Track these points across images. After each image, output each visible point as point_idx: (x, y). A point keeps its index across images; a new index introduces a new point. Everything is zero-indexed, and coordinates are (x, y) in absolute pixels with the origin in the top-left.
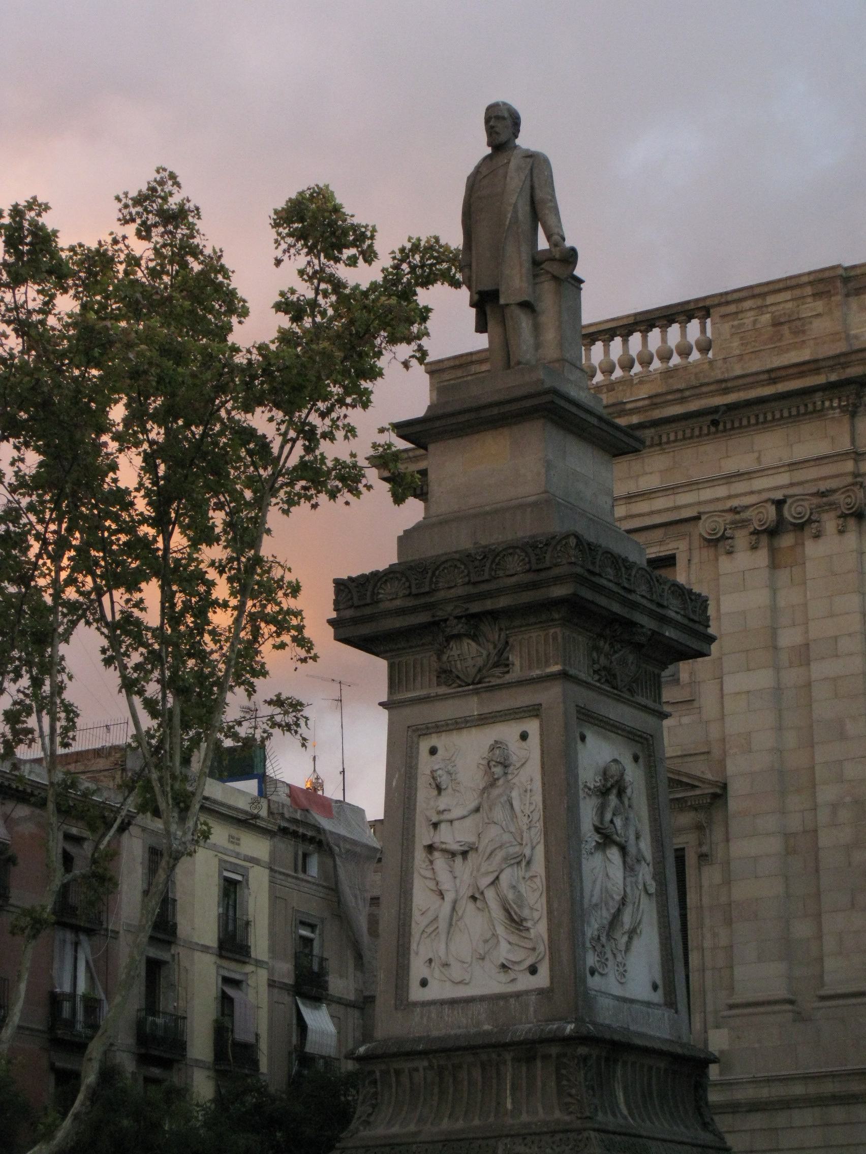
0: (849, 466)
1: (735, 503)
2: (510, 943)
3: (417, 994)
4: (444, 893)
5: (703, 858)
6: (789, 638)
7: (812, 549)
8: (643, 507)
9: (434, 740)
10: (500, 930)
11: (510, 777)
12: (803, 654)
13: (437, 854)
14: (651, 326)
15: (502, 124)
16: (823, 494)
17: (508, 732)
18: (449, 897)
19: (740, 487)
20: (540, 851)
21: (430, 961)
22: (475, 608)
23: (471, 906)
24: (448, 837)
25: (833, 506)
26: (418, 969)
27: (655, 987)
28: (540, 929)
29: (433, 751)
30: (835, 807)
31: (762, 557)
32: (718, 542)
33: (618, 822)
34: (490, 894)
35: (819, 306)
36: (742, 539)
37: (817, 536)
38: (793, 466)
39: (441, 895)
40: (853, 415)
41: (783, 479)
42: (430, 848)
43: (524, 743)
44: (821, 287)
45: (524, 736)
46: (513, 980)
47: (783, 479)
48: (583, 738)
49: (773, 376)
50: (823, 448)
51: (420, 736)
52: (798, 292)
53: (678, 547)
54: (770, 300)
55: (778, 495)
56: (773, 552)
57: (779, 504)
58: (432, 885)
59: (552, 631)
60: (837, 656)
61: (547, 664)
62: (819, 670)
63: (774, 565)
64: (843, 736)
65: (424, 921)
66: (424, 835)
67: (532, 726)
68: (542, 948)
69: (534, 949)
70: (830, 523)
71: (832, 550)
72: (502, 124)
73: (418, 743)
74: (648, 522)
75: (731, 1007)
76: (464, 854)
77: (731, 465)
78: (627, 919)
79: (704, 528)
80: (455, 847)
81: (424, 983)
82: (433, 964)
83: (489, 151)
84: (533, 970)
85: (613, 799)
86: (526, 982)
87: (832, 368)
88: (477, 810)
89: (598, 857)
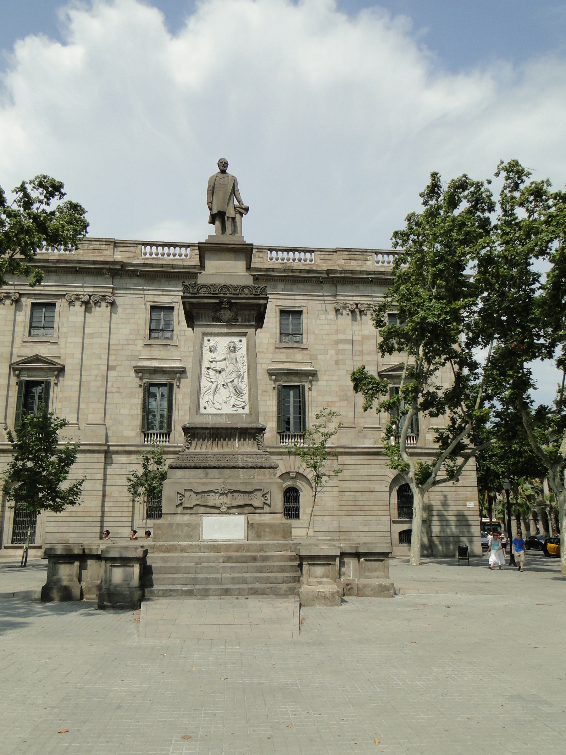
1: (77, 293)
3: (202, 410)
5: (56, 384)
10: (232, 395)
13: (210, 370)
15: (223, 166)
16: (103, 296)
17: (236, 339)
18: (215, 384)
20: (246, 375)
22: (233, 301)
23: (222, 388)
24: (218, 366)
25: (105, 299)
26: (203, 403)
28: (246, 397)
29: (209, 340)
30: (96, 376)
34: (229, 384)
35: (107, 247)
39: (212, 382)
40: (113, 278)
41: (92, 290)
42: (208, 368)
44: (108, 243)
46: (237, 410)
49: (95, 262)
52: (101, 243)
55: (90, 294)
59: (252, 312)
61: (250, 322)
64: (101, 358)
65: (205, 389)
66: (206, 364)
67: (244, 339)
68: (247, 402)
69: (244, 402)
72: (223, 166)
75: (88, 424)
76: (220, 372)
80: (218, 368)
81: (205, 408)
83: (219, 171)
86: (241, 411)
87: (111, 265)
88: (225, 359)
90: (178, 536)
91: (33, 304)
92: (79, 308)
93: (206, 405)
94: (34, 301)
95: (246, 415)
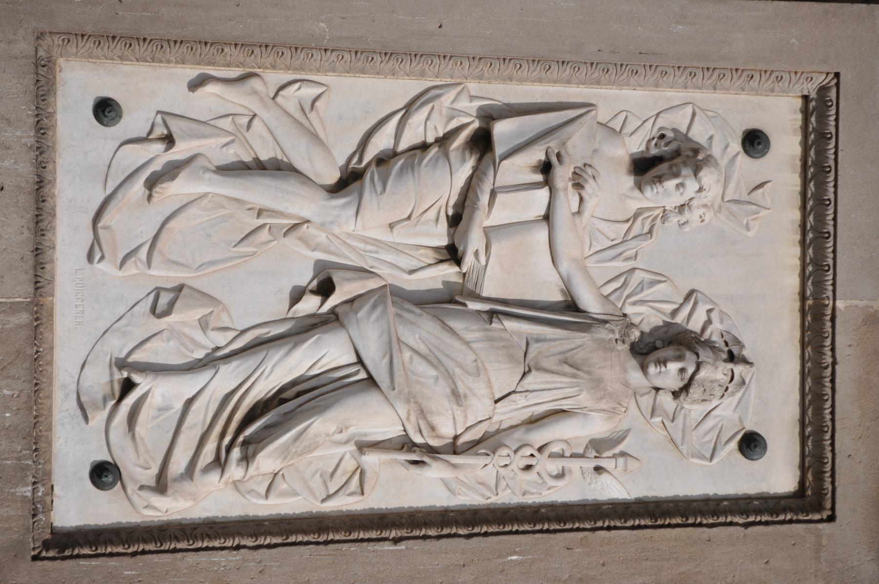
2: (190, 402)
4: (355, 185)
9: (787, 145)
11: (646, 402)
21: (169, 140)
39: (349, 181)
43: (734, 445)
51: (806, 98)
58: (382, 142)
73: (785, 92)
82: (160, 147)
84: (103, 473)
93: (134, 121)
95: (38, 507)
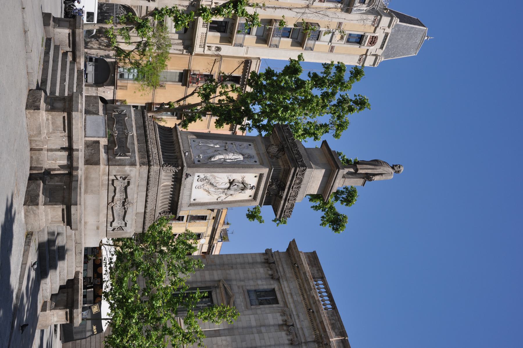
0: (303, 341)
1: (292, 316)
6: (263, 329)
7: (283, 334)
8: (289, 296)
12: (259, 332)
14: (329, 297)
16: (296, 335)
19: (296, 317)
27: (194, 200)
29: (250, 145)
31: (281, 322)
32: (283, 314)
33: (236, 187)
36: (285, 318)
37: (287, 335)
38: (302, 328)
45: (256, 162)
47: (299, 326)
48: (255, 177)
50: (307, 334)
53: (281, 304)
54: (338, 322)
56: (282, 325)
57: (293, 325)
60: (260, 340)
62: (257, 336)
63: (279, 325)
70: (290, 337)
71: (283, 337)
74: (286, 298)
77: (301, 315)
78: (212, 189)
79: (286, 309)
85: (241, 185)
89: (227, 181)
90: (89, 106)
91: (273, 290)
92: (279, 320)
94: (276, 289)
